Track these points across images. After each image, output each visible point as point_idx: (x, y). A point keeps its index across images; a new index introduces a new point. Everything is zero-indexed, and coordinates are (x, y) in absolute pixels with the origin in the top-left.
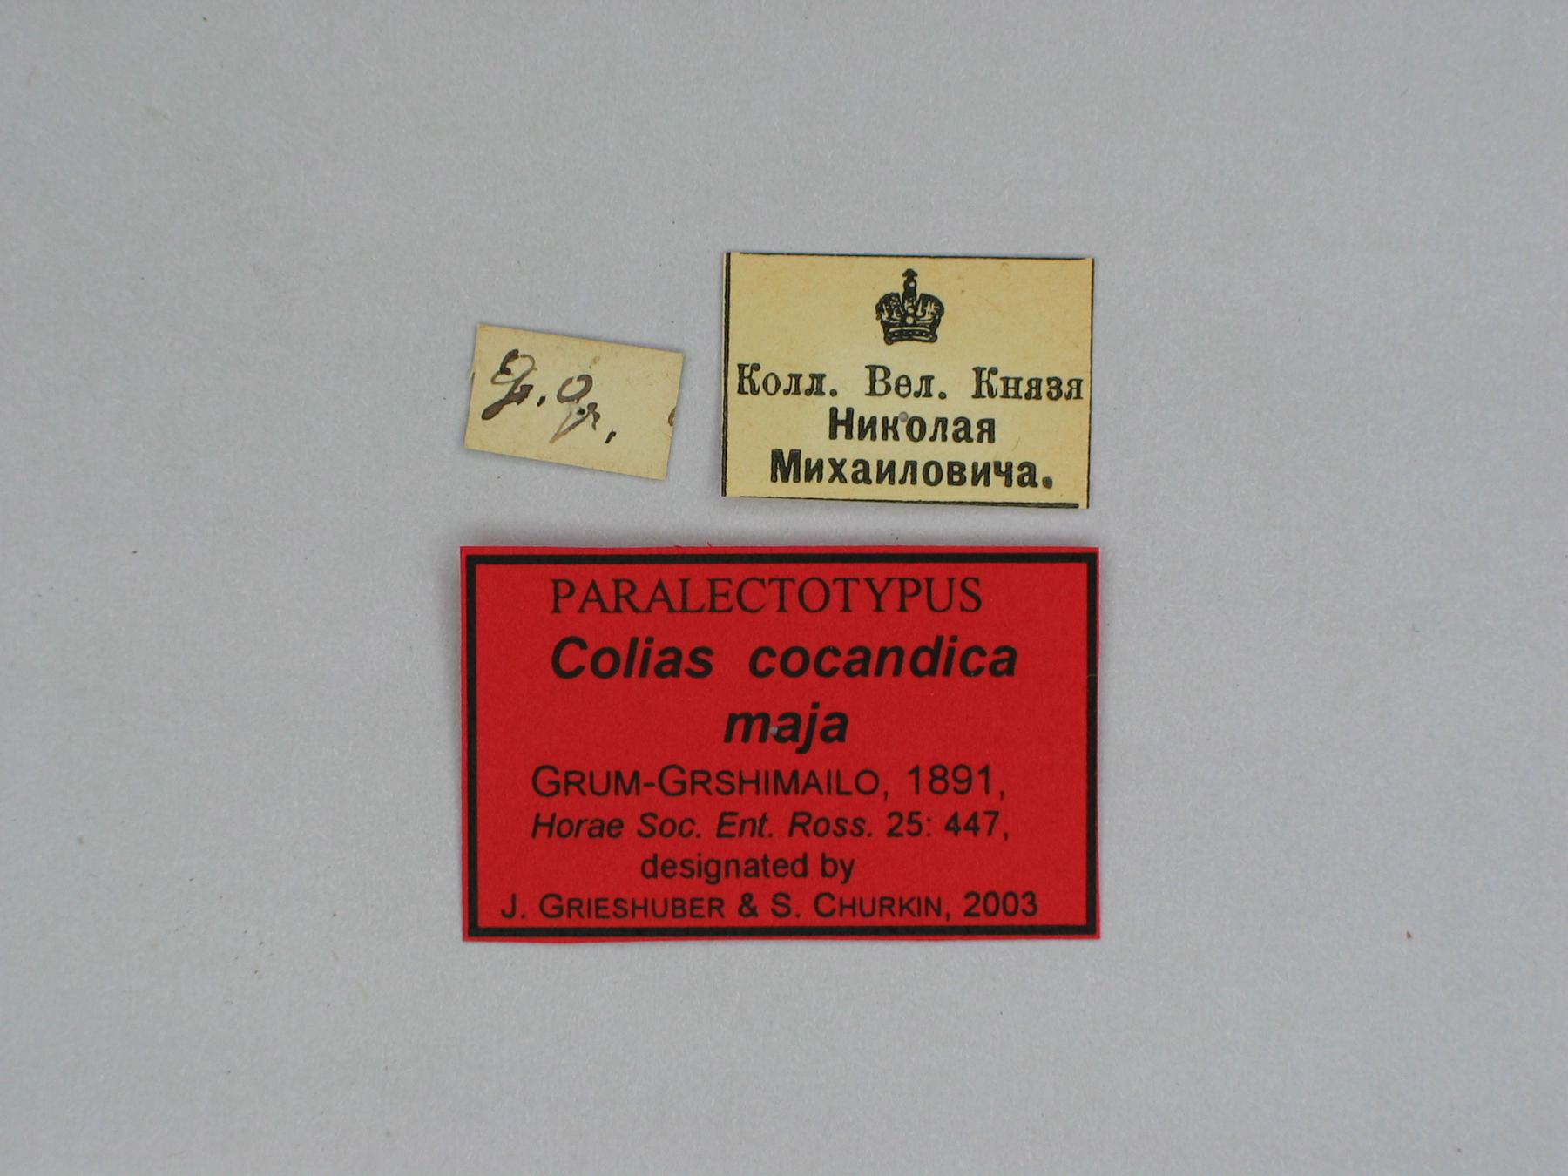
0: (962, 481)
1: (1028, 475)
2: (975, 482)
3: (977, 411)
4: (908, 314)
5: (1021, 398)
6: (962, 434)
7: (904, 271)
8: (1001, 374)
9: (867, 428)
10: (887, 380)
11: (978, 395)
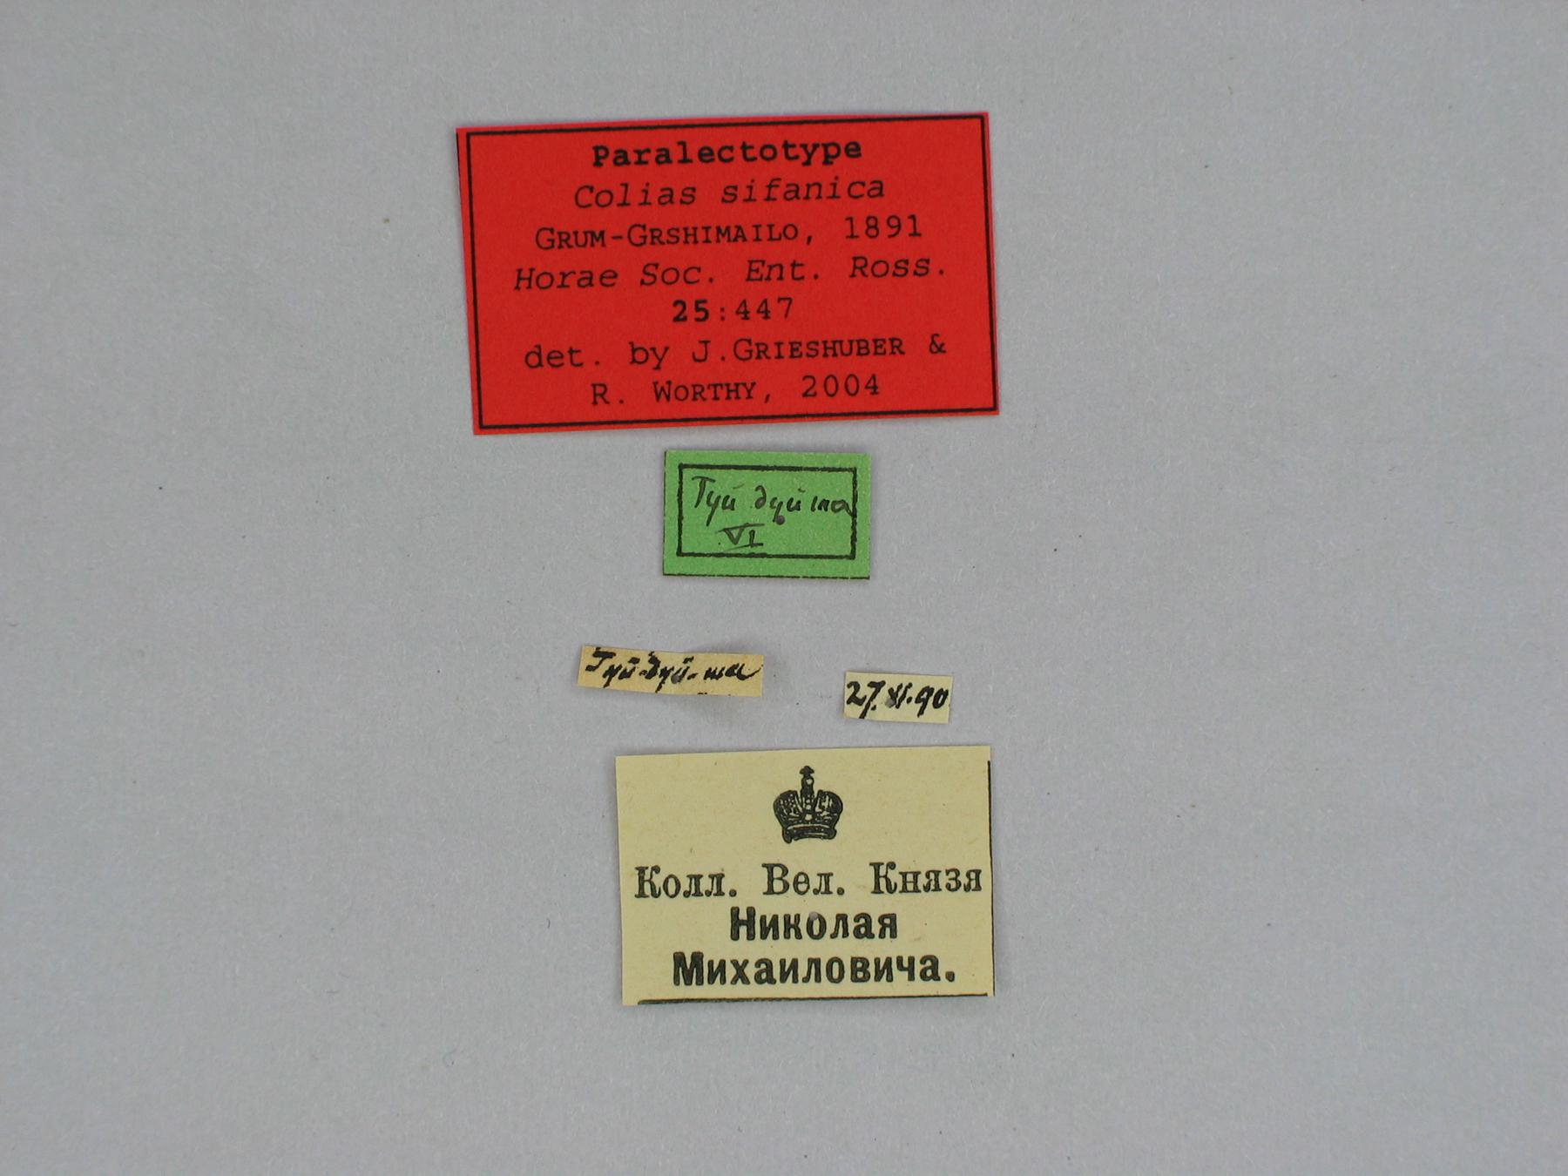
3: (878, 906)
10: (784, 878)
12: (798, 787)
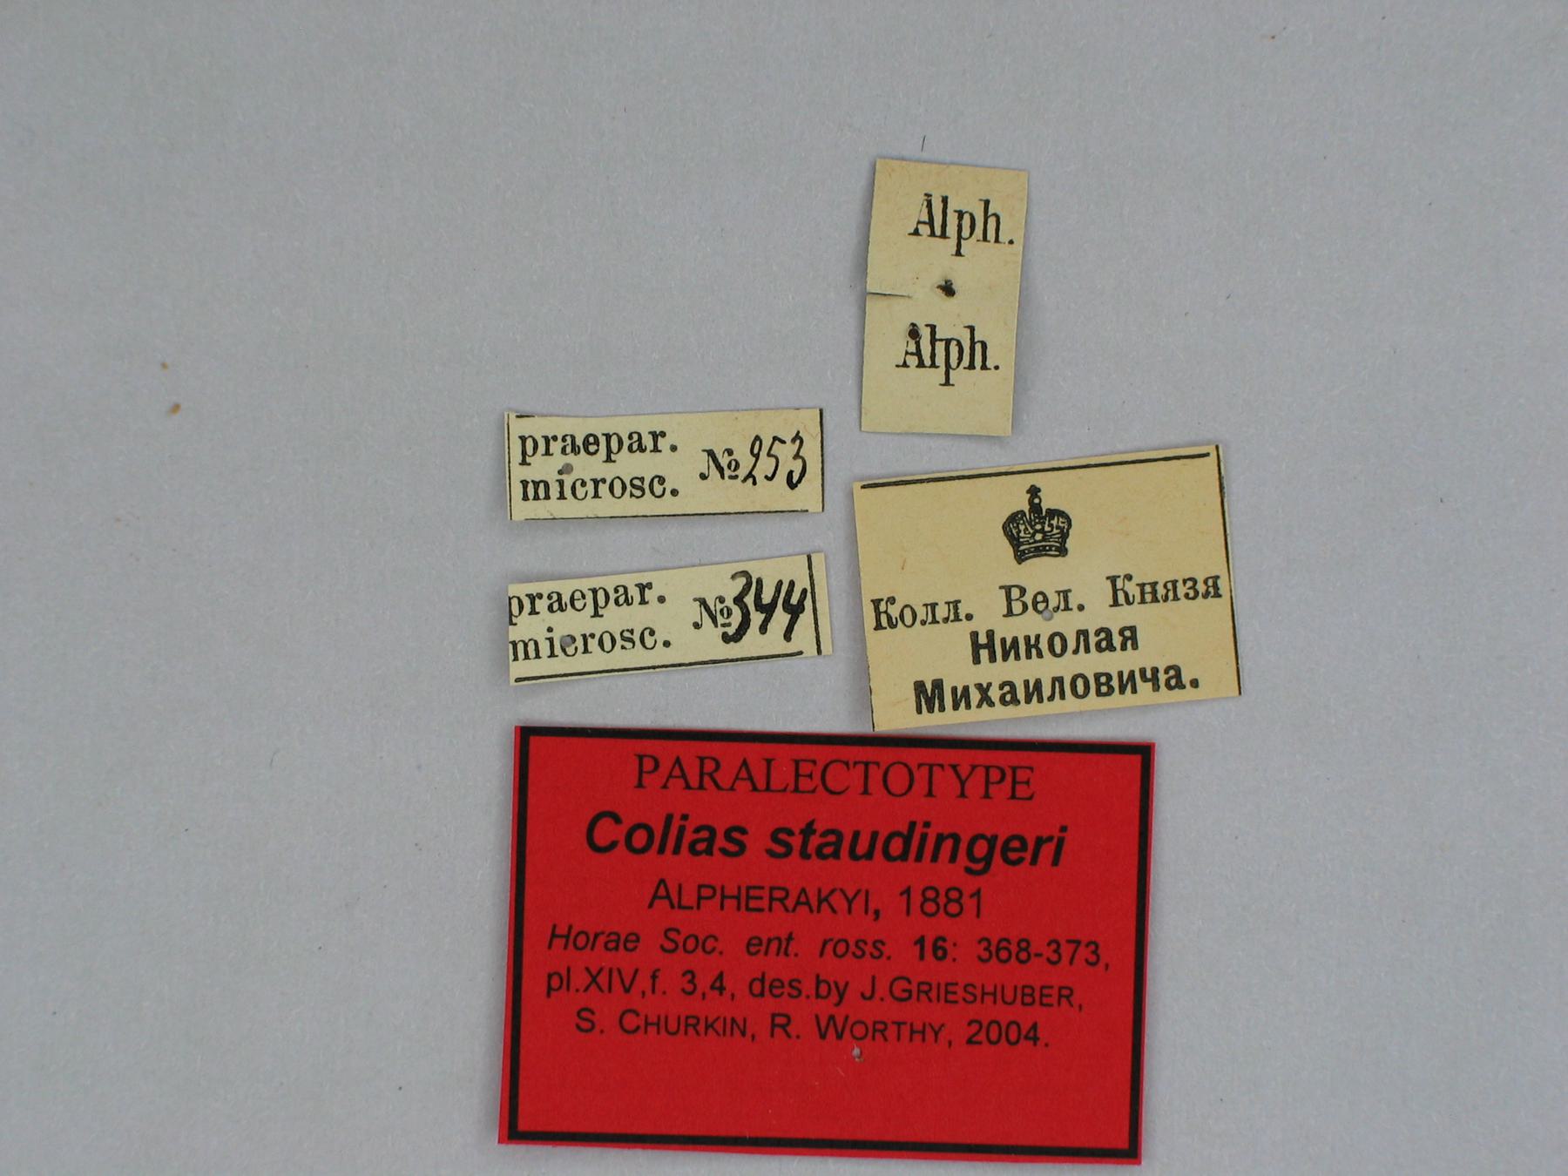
0: (1111, 690)
1: (1175, 678)
2: (1122, 690)
4: (1037, 531)
5: (1159, 601)
6: (1104, 644)
7: (1028, 487)
8: (1136, 580)
9: (1011, 649)
11: (1116, 603)
12: (1026, 508)
